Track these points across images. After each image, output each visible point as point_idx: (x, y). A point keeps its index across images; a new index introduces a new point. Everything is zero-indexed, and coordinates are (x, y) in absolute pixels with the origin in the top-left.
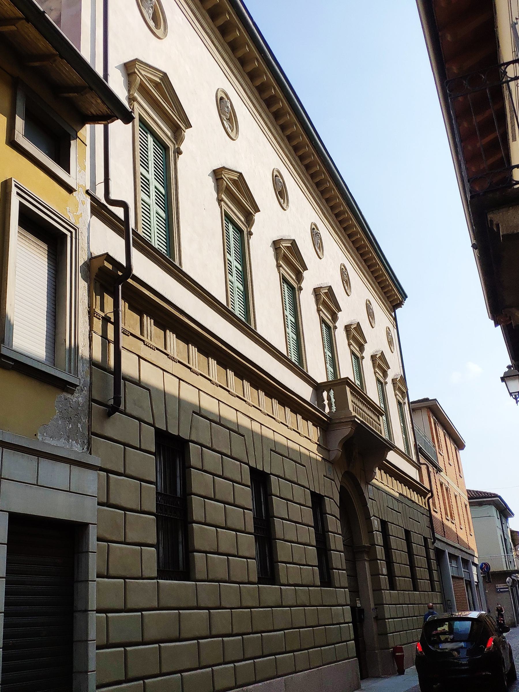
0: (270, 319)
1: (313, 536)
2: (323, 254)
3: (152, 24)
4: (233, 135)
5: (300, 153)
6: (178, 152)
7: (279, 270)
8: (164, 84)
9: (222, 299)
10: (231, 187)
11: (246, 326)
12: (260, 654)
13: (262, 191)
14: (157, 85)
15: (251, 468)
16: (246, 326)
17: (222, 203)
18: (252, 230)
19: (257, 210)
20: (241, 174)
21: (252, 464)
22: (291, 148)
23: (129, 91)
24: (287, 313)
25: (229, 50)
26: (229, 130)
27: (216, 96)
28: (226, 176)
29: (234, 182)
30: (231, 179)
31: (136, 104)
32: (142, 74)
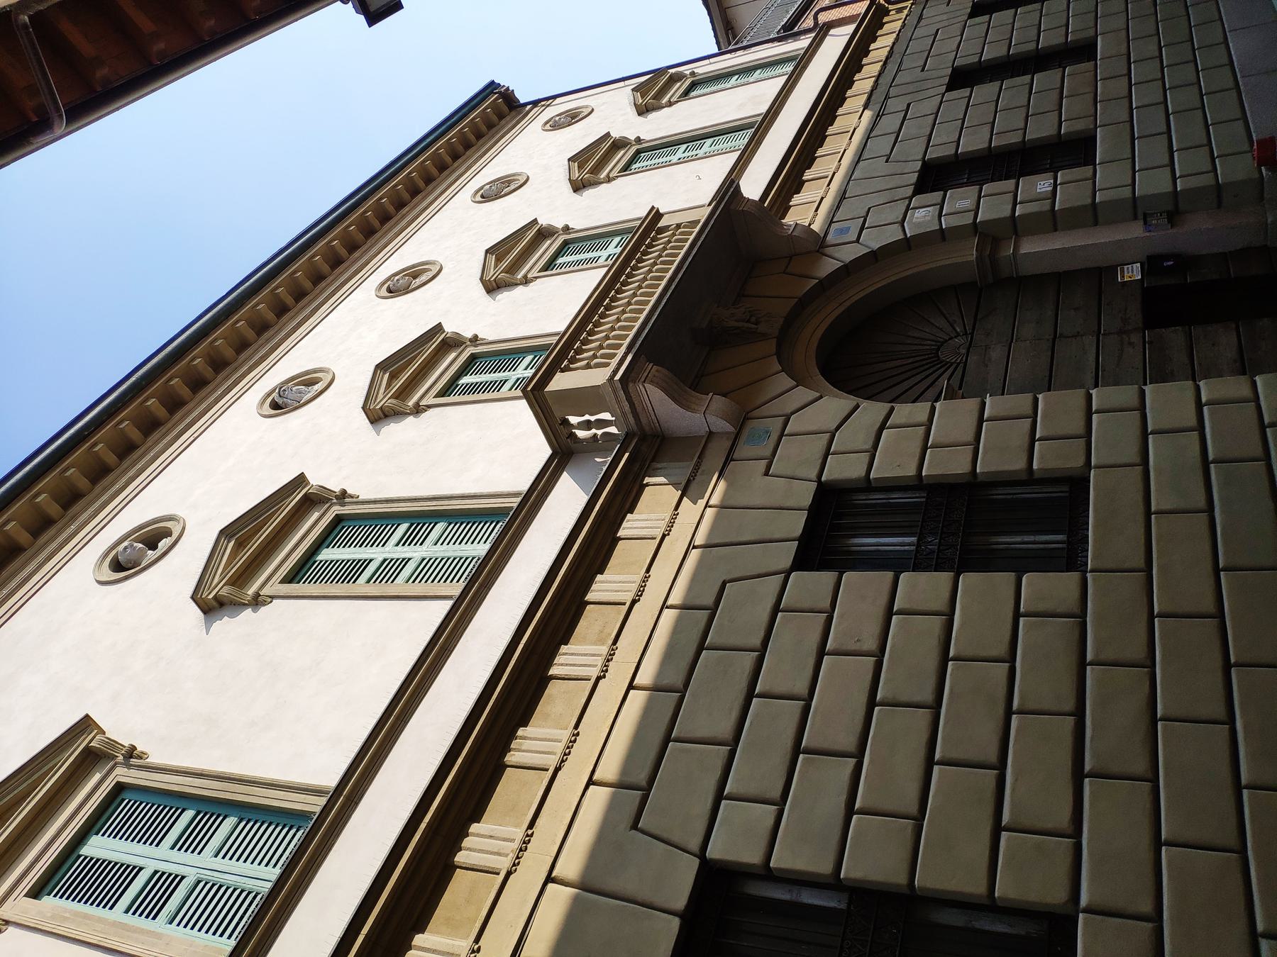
0: (750, 99)
1: (1030, 7)
2: (587, 107)
3: (318, 387)
4: (435, 269)
5: (448, 159)
6: (475, 340)
7: (614, 179)
8: (391, 366)
9: (783, 79)
10: (510, 262)
11: (761, 127)
12: (1192, 65)
13: (505, 218)
14: (393, 377)
15: (948, 90)
16: (761, 127)
17: (530, 276)
18: (633, 138)
19: (608, 135)
20: (487, 251)
21: (910, 191)
22: (456, 164)
23: (517, 285)
24: (674, 159)
25: (323, 284)
26: (430, 274)
27: (315, 371)
28: (491, 274)
29: (498, 260)
30: (496, 266)
31: (423, 403)
32: (384, 399)
